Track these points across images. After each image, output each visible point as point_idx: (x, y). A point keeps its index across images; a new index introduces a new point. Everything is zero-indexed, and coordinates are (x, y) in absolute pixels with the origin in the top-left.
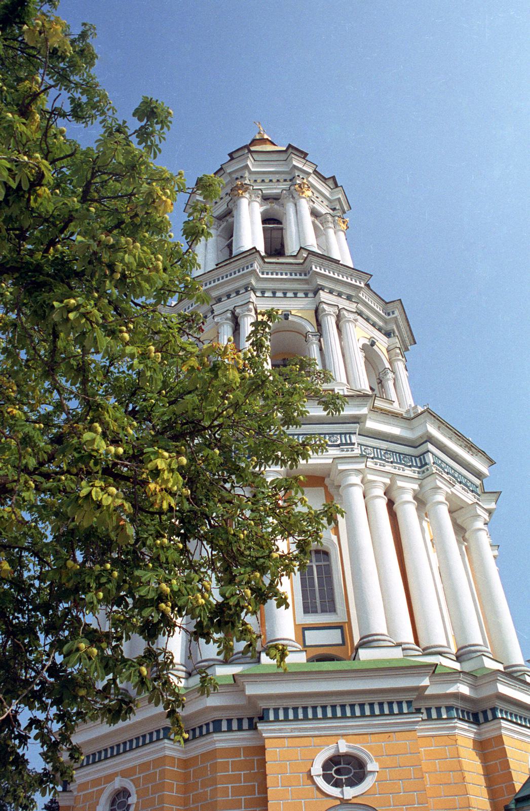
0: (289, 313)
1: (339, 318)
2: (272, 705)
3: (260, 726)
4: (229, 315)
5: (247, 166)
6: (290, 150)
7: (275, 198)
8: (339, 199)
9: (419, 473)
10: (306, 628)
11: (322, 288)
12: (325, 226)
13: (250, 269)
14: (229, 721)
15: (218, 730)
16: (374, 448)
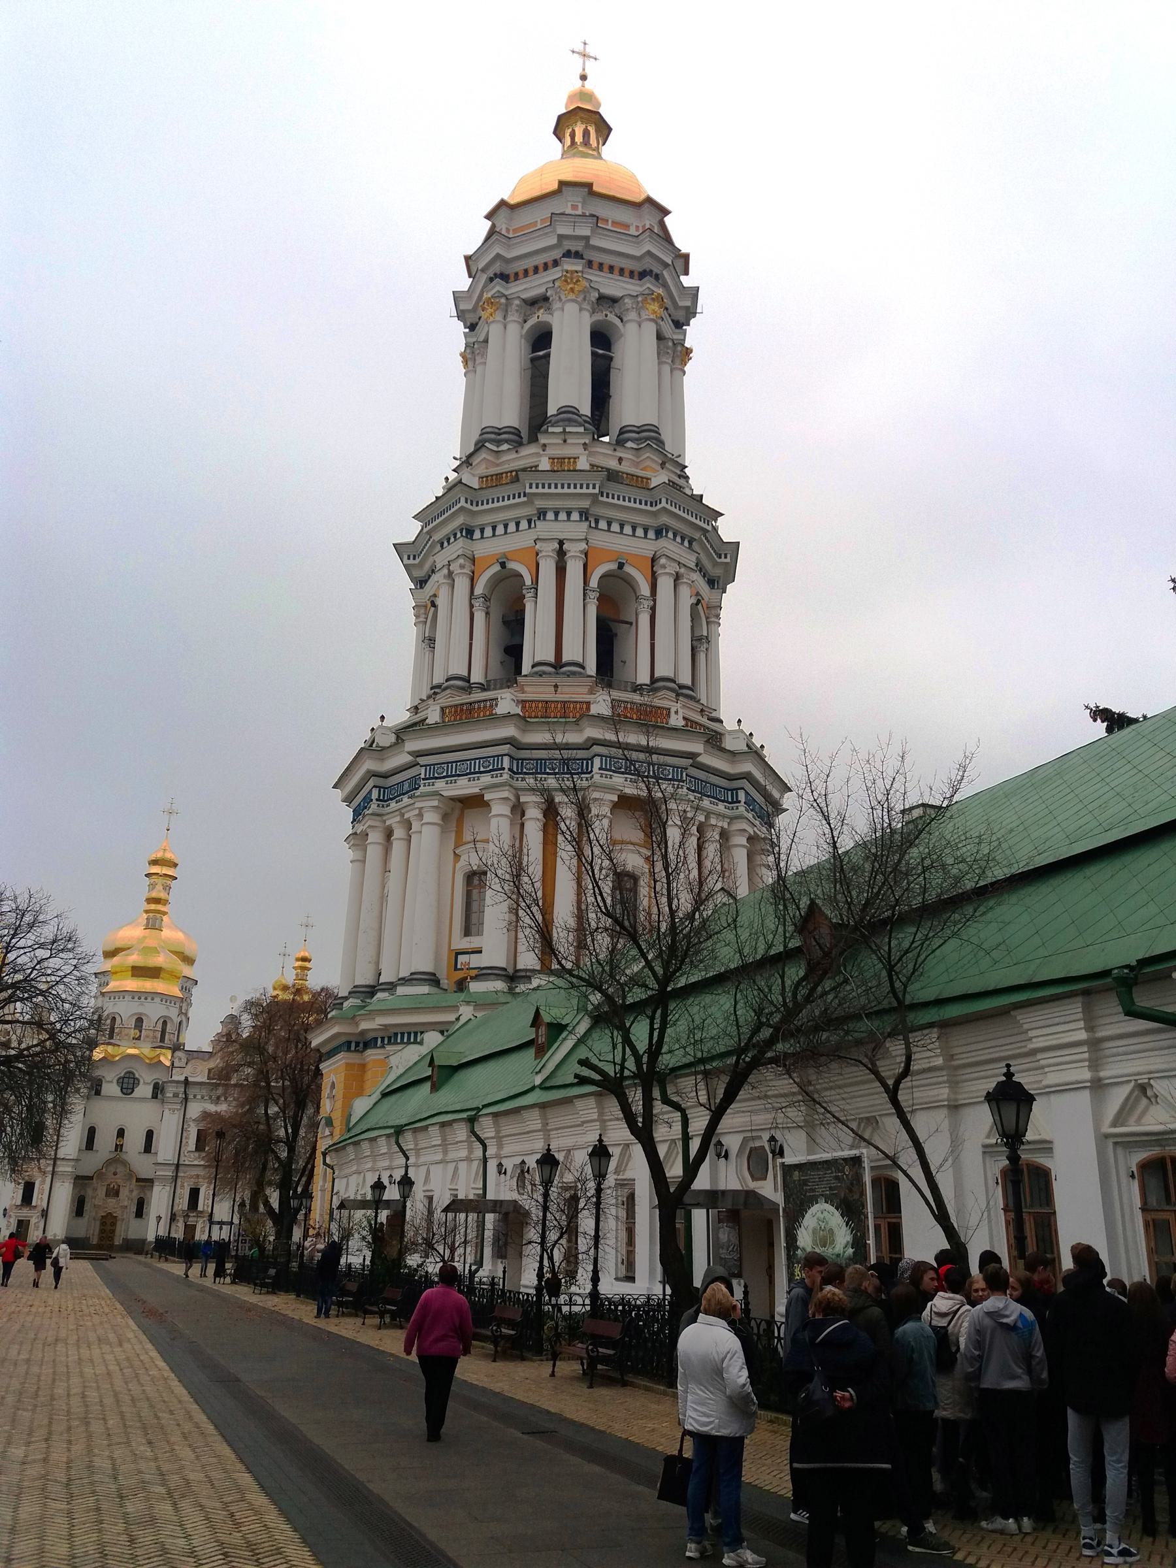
1: (561, 553)
2: (399, 1030)
3: (388, 1048)
4: (445, 571)
5: (498, 256)
6: (564, 188)
7: (545, 299)
8: (649, 253)
9: (587, 780)
10: (457, 954)
11: (542, 514)
12: (625, 319)
13: (459, 506)
14: (383, 1039)
15: (375, 1047)
16: (537, 760)
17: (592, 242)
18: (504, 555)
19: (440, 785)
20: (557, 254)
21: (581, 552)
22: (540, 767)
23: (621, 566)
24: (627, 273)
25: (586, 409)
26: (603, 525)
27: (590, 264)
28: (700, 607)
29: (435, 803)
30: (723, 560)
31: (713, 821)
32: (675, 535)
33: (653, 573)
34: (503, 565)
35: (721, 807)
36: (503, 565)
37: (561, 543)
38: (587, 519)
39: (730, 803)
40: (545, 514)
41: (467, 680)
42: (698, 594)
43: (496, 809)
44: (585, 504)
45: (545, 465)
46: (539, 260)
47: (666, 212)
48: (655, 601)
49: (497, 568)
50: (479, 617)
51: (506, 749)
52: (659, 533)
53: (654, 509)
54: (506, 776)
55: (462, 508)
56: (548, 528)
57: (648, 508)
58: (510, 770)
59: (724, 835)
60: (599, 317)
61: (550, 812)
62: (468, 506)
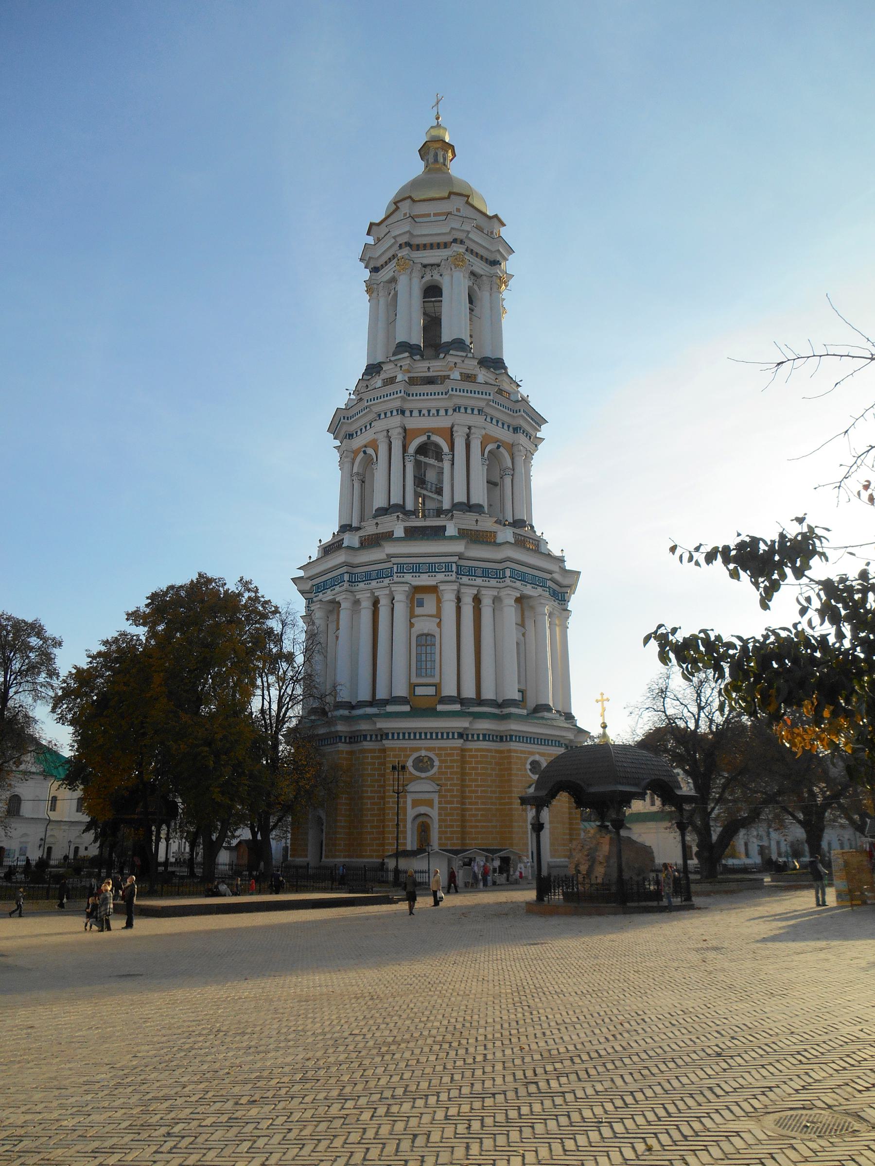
0: (363, 449)
8: (452, 229)
17: (415, 233)
18: (366, 447)
19: (321, 594)
20: (397, 247)
21: (399, 434)
22: (368, 577)
23: (429, 437)
24: (442, 246)
25: (417, 338)
26: (416, 413)
27: (418, 247)
28: (502, 449)
29: (319, 606)
30: (518, 414)
31: (483, 592)
32: (466, 409)
33: (452, 435)
34: (365, 452)
35: (493, 582)
36: (365, 452)
37: (388, 431)
38: (403, 412)
39: (500, 578)
40: (379, 415)
41: (350, 526)
42: (497, 440)
43: (343, 606)
44: (398, 404)
45: (379, 383)
46: (389, 254)
47: (468, 197)
48: (453, 455)
49: (361, 455)
50: (357, 485)
51: (344, 569)
52: (455, 410)
53: (447, 396)
54: (346, 585)
55: (343, 423)
56: (380, 425)
57: (444, 396)
58: (348, 581)
59: (497, 600)
60: (427, 278)
61: (376, 603)
62: (346, 420)
